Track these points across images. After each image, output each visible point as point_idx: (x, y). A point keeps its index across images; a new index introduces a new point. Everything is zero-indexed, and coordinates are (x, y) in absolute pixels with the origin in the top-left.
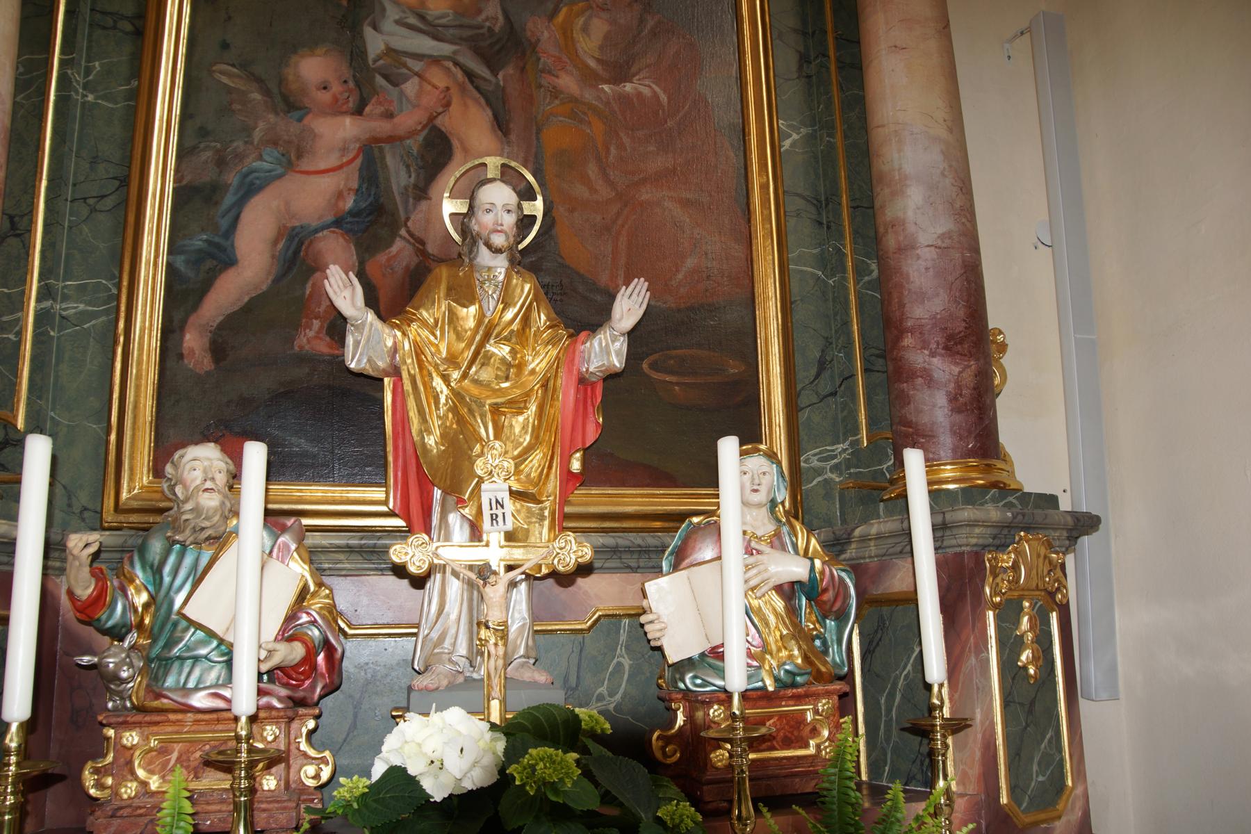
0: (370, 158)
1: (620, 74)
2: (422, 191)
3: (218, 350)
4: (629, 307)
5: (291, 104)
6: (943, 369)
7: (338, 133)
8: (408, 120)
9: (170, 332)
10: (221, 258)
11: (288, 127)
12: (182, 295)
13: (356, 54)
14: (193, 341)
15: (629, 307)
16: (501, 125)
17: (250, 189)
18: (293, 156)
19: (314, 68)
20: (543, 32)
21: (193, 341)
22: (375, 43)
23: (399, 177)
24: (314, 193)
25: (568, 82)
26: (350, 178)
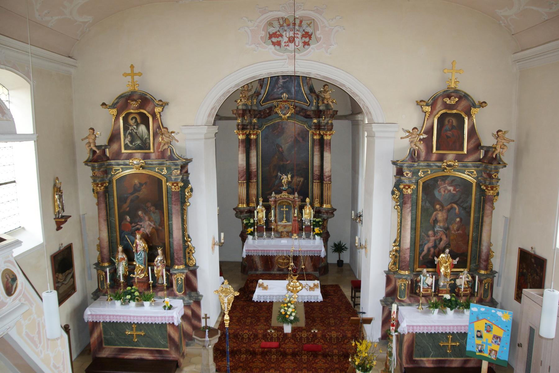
0: (435, 241)
1: (458, 230)
2: (439, 244)
3: (423, 258)
4: (457, 259)
5: (428, 236)
6: (484, 263)
7: (432, 239)
8: (438, 237)
9: (419, 257)
10: (423, 250)
11: (428, 238)
12: (420, 254)
13: (434, 231)
14: (421, 257)
15: (457, 259)
16: (447, 237)
17: (425, 244)
18: (429, 241)
19: (430, 233)
20: (451, 227)
21: (421, 257)
22: (436, 230)
23: (437, 242)
24: (430, 244)
25: (453, 232)
26: (433, 243)
